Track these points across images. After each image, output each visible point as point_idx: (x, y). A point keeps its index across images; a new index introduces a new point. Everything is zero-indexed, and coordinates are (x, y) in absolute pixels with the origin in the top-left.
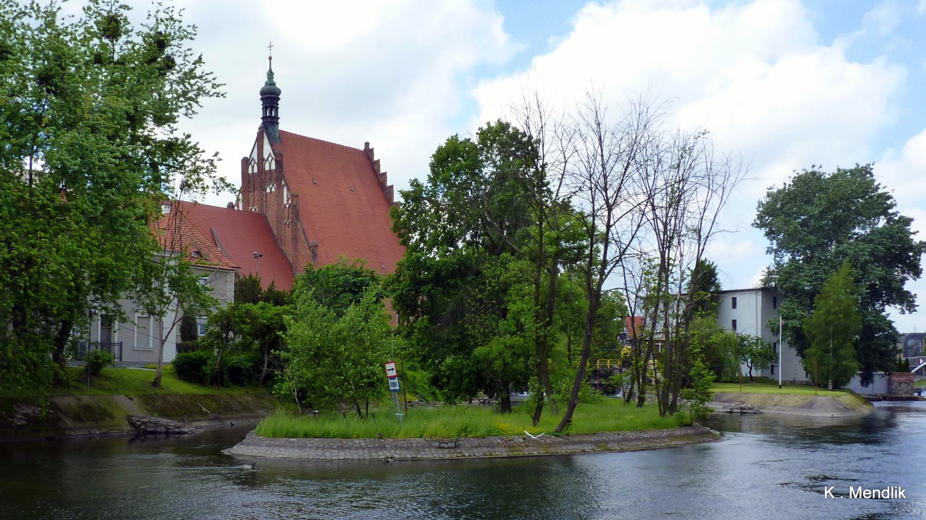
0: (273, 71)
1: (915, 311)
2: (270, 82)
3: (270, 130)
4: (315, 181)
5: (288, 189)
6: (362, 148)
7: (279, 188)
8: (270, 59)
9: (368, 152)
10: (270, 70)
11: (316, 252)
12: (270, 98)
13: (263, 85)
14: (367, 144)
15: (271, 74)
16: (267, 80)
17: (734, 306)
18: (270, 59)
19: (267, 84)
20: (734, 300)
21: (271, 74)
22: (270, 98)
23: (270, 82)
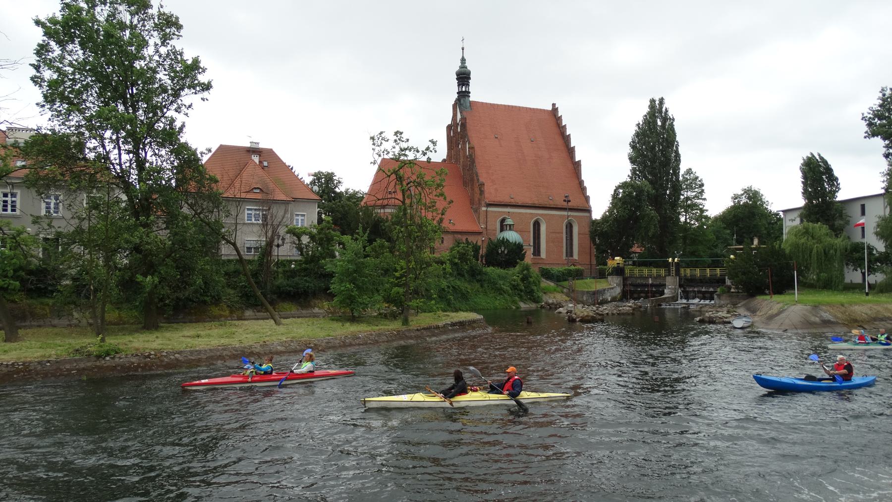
1: (735, 195)
3: (462, 101)
4: (496, 136)
5: (469, 144)
7: (464, 143)
8: (463, 49)
9: (555, 110)
10: (463, 57)
11: (483, 189)
12: (463, 77)
14: (554, 105)
15: (463, 60)
17: (863, 213)
18: (463, 49)
19: (461, 67)
20: (863, 206)
21: (463, 60)
22: (463, 77)
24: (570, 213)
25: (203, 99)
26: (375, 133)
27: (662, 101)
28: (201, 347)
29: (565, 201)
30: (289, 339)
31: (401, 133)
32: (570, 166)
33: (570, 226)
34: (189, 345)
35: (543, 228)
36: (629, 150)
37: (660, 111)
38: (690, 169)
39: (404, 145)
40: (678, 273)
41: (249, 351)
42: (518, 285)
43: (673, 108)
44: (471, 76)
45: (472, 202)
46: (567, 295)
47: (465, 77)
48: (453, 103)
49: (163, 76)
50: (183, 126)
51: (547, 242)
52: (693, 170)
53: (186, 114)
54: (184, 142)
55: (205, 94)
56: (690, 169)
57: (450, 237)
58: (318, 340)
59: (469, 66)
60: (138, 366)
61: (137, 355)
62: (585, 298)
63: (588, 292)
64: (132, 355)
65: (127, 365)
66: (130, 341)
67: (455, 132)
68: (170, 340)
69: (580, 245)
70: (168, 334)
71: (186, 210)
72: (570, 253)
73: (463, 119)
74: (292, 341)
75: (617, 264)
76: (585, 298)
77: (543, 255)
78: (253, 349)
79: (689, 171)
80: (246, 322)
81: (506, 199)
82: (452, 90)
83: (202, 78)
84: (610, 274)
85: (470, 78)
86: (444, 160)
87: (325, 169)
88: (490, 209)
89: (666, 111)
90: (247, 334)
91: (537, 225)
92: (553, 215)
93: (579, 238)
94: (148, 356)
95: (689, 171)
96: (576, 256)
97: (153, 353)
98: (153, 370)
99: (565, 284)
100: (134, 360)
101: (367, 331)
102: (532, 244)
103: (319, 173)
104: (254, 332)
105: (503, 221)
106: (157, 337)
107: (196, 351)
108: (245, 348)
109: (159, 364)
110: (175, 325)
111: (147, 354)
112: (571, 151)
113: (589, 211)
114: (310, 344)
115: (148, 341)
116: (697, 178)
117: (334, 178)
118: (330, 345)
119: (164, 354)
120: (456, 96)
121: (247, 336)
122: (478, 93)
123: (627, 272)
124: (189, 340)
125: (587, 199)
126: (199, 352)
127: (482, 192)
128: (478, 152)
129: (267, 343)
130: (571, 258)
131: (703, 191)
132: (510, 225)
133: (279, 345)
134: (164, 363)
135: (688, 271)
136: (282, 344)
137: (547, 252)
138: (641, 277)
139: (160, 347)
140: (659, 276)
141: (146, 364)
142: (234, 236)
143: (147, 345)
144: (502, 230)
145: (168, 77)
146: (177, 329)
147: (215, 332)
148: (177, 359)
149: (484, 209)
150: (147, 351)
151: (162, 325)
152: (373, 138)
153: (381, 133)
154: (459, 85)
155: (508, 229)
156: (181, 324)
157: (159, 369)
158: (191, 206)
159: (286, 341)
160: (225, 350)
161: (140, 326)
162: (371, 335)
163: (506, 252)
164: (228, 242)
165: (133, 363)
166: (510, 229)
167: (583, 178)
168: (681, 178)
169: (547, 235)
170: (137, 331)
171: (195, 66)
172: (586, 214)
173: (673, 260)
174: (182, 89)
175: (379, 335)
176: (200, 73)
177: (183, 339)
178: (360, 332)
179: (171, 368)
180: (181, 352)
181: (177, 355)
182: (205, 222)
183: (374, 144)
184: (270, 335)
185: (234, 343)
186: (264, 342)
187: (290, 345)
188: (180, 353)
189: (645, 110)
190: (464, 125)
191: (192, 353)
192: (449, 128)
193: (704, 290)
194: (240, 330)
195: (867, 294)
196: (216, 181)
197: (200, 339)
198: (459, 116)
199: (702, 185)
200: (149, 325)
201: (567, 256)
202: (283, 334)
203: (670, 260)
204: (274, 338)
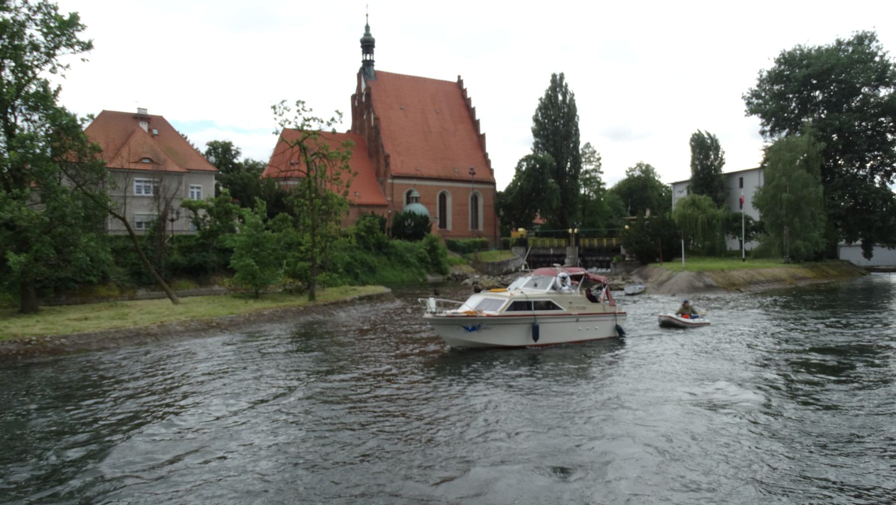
0: (370, 25)
2: (367, 34)
3: (367, 70)
5: (374, 114)
7: (369, 114)
8: (367, 15)
9: (460, 82)
12: (368, 45)
13: (362, 36)
14: (459, 77)
15: (367, 28)
17: (741, 186)
20: (741, 180)
21: (367, 28)
22: (368, 45)
23: (367, 34)
24: (475, 186)
25: (83, 60)
26: (277, 103)
27: (562, 76)
28: (90, 330)
29: (470, 173)
30: (189, 319)
31: (303, 103)
32: (475, 138)
33: (475, 199)
34: (77, 329)
35: (449, 201)
36: (532, 124)
37: (561, 86)
38: (589, 143)
39: (307, 115)
40: (577, 243)
41: (145, 332)
42: (425, 257)
43: (572, 84)
44: (376, 44)
45: (378, 174)
46: (473, 267)
47: (369, 46)
48: (357, 71)
49: (34, 32)
50: (59, 89)
51: (453, 215)
52: (592, 145)
53: (63, 76)
54: (61, 106)
55: (86, 54)
56: (589, 143)
57: (356, 210)
58: (221, 319)
59: (374, 34)
60: (18, 353)
61: (15, 342)
62: (490, 269)
63: (493, 264)
64: (10, 342)
65: (4, 353)
66: (6, 327)
67: (360, 102)
68: (53, 324)
69: (485, 217)
70: (50, 318)
71: (66, 183)
72: (475, 225)
73: (368, 89)
74: (192, 321)
77: (449, 227)
78: (149, 331)
79: (588, 145)
80: (139, 302)
81: (412, 171)
82: (357, 59)
83: (81, 36)
84: (515, 245)
85: (373, 46)
86: (349, 132)
87: (221, 138)
88: (397, 181)
89: (566, 85)
90: (142, 314)
91: (443, 197)
92: (459, 188)
93: (484, 211)
94: (29, 343)
95: (588, 145)
96: (481, 228)
97: (34, 338)
98: (35, 357)
99: (471, 255)
100: (11, 347)
101: (272, 308)
102: (438, 216)
103: (216, 142)
104: (149, 313)
105: (409, 193)
106: (38, 321)
107: (85, 335)
108: (140, 329)
109: (42, 350)
110: (58, 308)
111: (27, 340)
112: (476, 124)
113: (493, 183)
114: (212, 322)
115: (28, 326)
116: (595, 152)
117: (232, 148)
118: (233, 323)
119: (48, 339)
120: (361, 65)
121: (143, 316)
123: (530, 242)
124: (76, 323)
125: (491, 172)
126: (88, 336)
127: (387, 164)
128: (383, 124)
129: (165, 323)
130: (476, 230)
131: (600, 164)
132: (416, 198)
133: (178, 325)
134: (48, 349)
135: (587, 241)
136: (181, 324)
137: (453, 224)
138: (543, 248)
139: (42, 332)
140: (559, 247)
141: (26, 351)
142: (123, 210)
143: (26, 330)
144: (409, 201)
145: (40, 33)
146: (60, 312)
147: (105, 313)
148: (63, 344)
149: (390, 181)
150: (27, 336)
151: (41, 307)
152: (274, 107)
153: (283, 102)
155: (414, 200)
156: (65, 306)
157: (43, 355)
158: (71, 178)
159: (185, 321)
160: (117, 332)
161: (17, 309)
162: (277, 311)
163: (413, 224)
164: (116, 216)
165: (11, 351)
166: (417, 202)
167: (488, 150)
168: (581, 152)
169: (453, 207)
170: (12, 315)
171: (73, 22)
172: (491, 187)
173: (573, 231)
174: (57, 47)
175: (285, 311)
176: (79, 31)
177: (67, 322)
178: (265, 309)
179: (56, 354)
180: (68, 336)
181: (63, 340)
182: (89, 196)
183: (275, 113)
184: (168, 315)
185: (129, 324)
186: (162, 322)
187: (190, 325)
188: (66, 337)
189: (548, 84)
190: (368, 95)
191: (80, 336)
192: (354, 98)
193: (601, 258)
194: (134, 311)
195: (744, 260)
196: (100, 151)
197: (88, 322)
198: (363, 86)
199: (599, 159)
200: (27, 309)
201: (472, 227)
202: (181, 314)
203: (570, 231)
204: (172, 318)
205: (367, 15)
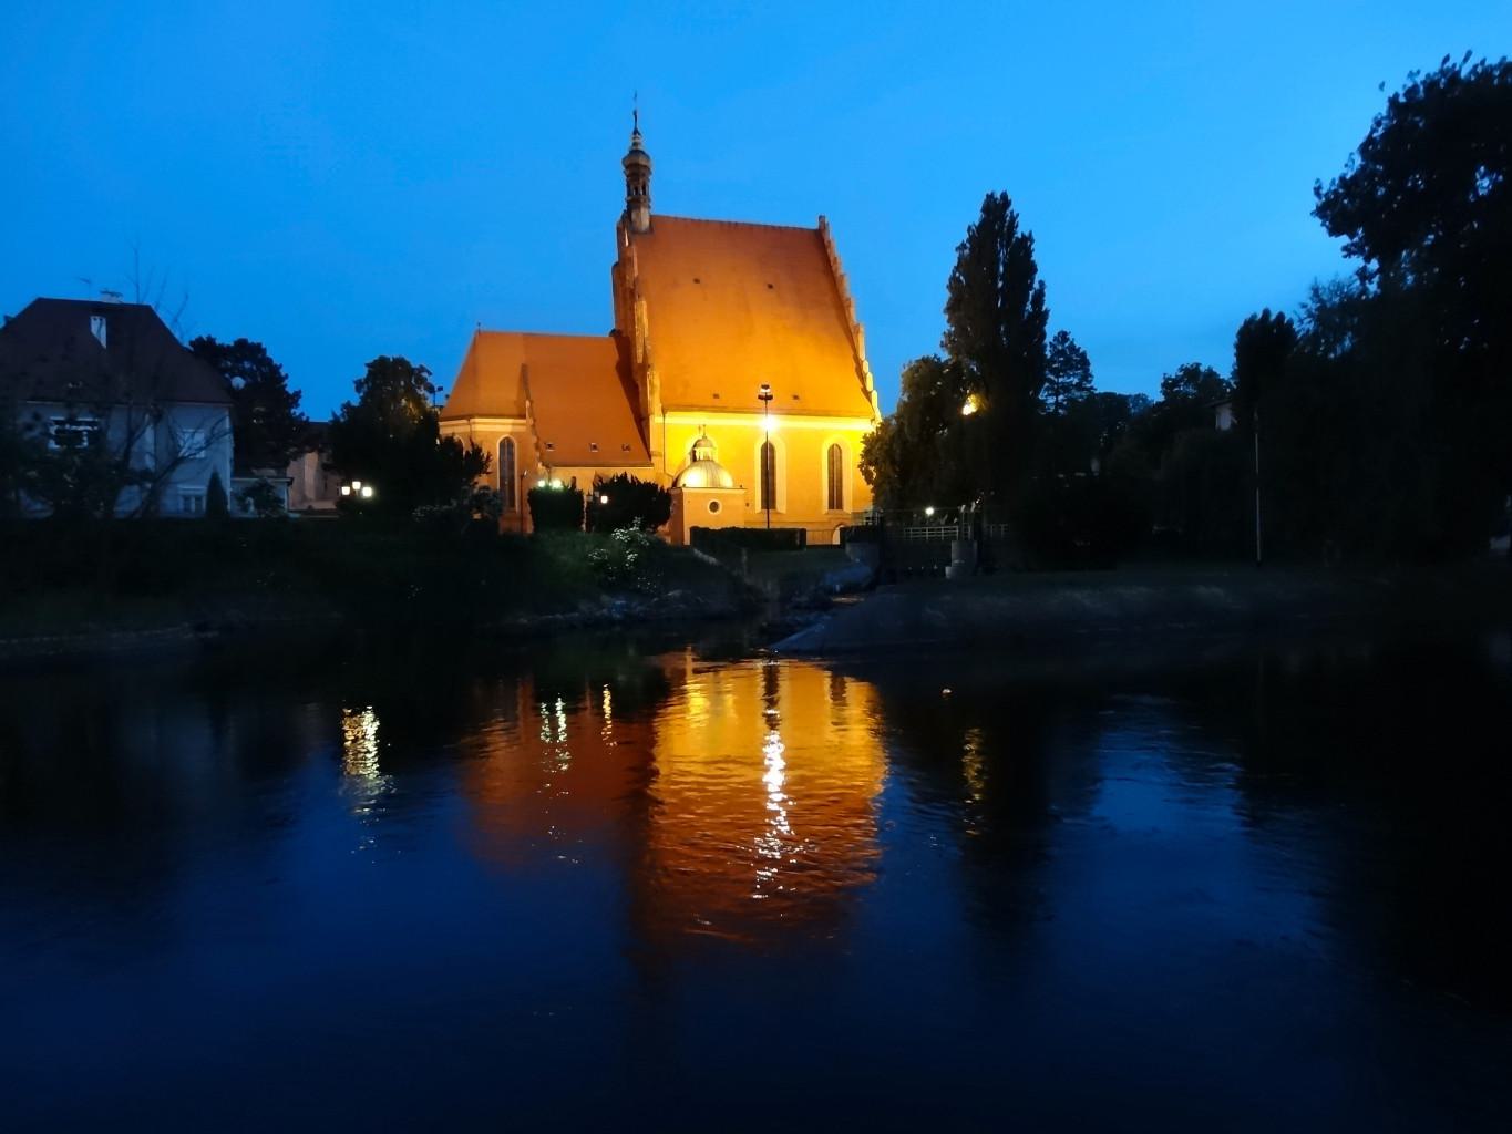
2: (636, 152)
3: (634, 216)
6: (815, 225)
8: (635, 113)
12: (637, 170)
16: (630, 143)
22: (637, 170)
23: (636, 152)
52: (1071, 337)
75: (868, 519)
76: (769, 588)
79: (1063, 336)
89: (1013, 219)
91: (768, 452)
95: (1063, 336)
116: (1073, 349)
120: (624, 206)
122: (664, 200)
154: (628, 186)
168: (1048, 354)
201: (831, 506)
205: (635, 113)
